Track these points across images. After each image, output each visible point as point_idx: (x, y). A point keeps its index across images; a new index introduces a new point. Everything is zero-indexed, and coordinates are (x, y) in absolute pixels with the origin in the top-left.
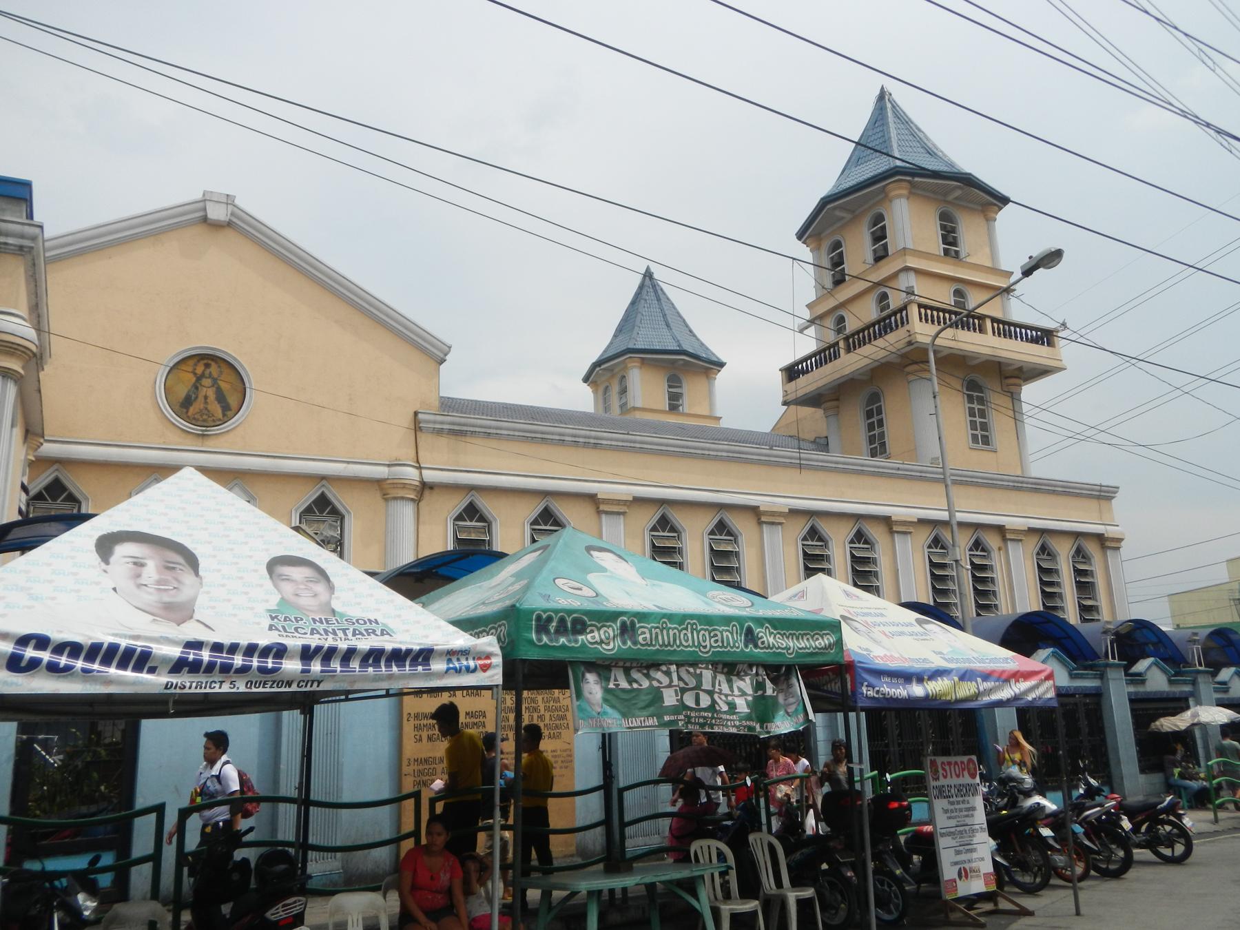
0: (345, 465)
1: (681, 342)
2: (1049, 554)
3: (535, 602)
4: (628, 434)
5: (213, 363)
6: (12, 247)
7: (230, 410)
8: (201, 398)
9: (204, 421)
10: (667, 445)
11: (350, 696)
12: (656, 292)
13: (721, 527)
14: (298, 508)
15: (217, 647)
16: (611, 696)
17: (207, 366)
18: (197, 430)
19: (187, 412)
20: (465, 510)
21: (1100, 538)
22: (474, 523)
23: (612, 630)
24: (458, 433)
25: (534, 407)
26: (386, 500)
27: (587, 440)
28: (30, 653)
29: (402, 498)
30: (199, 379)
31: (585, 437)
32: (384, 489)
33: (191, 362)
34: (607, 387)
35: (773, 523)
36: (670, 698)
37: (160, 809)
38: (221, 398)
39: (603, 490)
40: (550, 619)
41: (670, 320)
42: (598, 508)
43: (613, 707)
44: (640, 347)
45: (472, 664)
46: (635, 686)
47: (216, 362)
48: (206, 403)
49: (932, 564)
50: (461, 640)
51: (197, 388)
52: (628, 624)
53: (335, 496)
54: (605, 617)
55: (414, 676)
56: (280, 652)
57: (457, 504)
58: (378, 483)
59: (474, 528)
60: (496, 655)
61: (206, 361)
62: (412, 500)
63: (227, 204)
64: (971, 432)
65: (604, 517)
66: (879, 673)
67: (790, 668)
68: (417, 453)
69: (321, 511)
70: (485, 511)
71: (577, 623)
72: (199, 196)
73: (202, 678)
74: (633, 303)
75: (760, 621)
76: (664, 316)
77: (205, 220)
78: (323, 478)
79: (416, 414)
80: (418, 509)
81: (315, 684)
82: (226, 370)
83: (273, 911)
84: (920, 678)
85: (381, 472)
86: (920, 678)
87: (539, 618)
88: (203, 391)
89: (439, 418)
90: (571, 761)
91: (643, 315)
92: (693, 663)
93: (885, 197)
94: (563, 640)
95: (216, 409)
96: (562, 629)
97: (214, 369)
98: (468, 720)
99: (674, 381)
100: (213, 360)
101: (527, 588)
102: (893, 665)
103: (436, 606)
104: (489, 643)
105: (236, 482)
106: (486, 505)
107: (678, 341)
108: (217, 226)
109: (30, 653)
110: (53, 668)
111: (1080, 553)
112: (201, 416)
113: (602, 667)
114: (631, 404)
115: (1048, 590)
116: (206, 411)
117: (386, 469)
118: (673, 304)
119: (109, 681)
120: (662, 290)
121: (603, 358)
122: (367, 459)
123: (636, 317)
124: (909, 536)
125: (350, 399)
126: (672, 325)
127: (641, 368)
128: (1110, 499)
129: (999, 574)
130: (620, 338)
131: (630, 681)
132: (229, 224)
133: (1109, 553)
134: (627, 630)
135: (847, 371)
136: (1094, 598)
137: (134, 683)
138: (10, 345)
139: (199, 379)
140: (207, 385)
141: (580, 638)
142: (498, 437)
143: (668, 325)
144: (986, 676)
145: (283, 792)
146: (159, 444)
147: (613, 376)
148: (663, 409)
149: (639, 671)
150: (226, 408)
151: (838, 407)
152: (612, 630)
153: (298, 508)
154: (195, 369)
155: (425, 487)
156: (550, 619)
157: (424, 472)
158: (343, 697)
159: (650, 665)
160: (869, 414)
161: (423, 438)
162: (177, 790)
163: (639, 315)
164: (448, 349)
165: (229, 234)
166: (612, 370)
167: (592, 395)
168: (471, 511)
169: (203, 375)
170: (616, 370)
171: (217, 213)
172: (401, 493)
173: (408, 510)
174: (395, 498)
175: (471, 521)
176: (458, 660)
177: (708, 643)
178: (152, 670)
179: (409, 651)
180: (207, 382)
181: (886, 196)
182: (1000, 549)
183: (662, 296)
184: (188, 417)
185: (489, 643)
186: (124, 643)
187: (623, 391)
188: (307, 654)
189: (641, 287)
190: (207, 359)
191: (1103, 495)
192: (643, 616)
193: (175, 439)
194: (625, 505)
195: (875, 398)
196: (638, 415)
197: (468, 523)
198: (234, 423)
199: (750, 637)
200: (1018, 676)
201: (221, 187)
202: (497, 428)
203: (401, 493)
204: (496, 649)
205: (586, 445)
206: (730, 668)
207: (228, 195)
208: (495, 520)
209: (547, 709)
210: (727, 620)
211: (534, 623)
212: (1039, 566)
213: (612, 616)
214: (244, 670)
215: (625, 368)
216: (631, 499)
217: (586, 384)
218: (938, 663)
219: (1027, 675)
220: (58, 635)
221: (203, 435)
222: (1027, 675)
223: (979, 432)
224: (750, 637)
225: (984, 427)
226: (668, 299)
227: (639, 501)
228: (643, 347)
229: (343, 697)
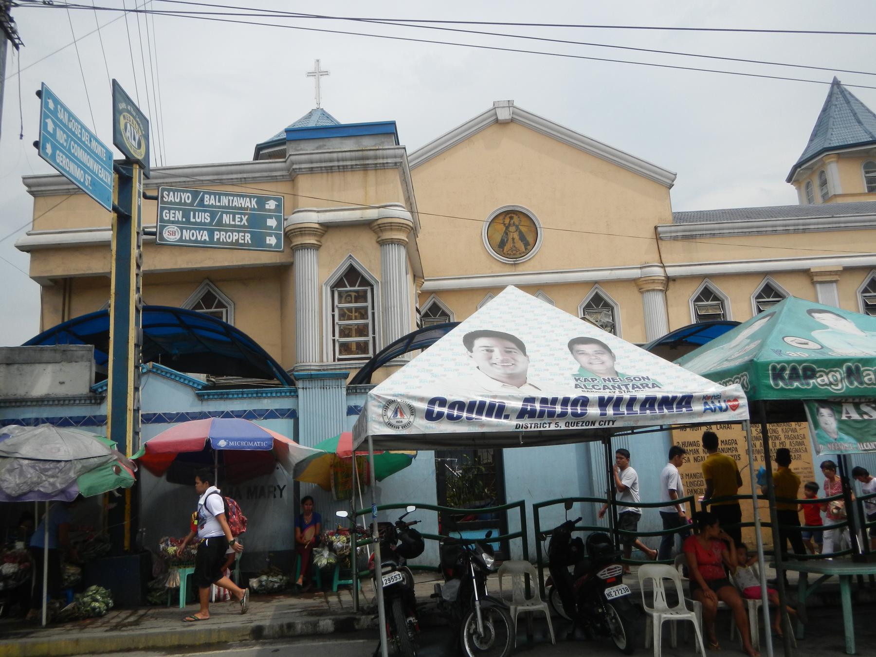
0: (609, 272)
1: (874, 133)
3: (769, 356)
4: (832, 217)
5: (514, 216)
6: (391, 165)
7: (529, 245)
8: (510, 240)
9: (514, 254)
10: (870, 221)
11: (635, 431)
12: (844, 96)
14: (582, 304)
15: (544, 401)
16: (845, 426)
17: (511, 218)
18: (511, 261)
19: (503, 251)
20: (702, 293)
22: (710, 303)
23: (839, 374)
24: (689, 237)
25: (748, 209)
26: (642, 293)
27: (796, 227)
28: (437, 409)
29: (654, 290)
30: (507, 228)
31: (794, 225)
32: (640, 285)
33: (501, 218)
34: (808, 183)
37: (522, 504)
38: (522, 238)
39: (814, 265)
40: (783, 369)
41: (861, 118)
42: (812, 279)
43: (847, 434)
44: (835, 145)
45: (723, 405)
46: (866, 417)
47: (517, 215)
48: (514, 242)
50: (713, 388)
51: (507, 234)
53: (607, 296)
55: (681, 415)
56: (584, 402)
57: (696, 289)
58: (635, 281)
59: (711, 306)
60: (742, 398)
61: (510, 215)
62: (661, 290)
63: (509, 107)
65: (818, 286)
68: (660, 256)
69: (597, 306)
70: (717, 292)
71: (808, 370)
72: (491, 106)
73: (537, 421)
74: (825, 110)
76: (855, 114)
77: (497, 121)
78: (596, 282)
79: (656, 228)
80: (666, 296)
81: (611, 423)
82: (524, 219)
83: (601, 572)
85: (636, 273)
87: (774, 368)
88: (510, 237)
89: (673, 228)
90: (812, 477)
91: (834, 118)
94: (796, 384)
95: (520, 245)
96: (794, 375)
97: (516, 220)
98: (723, 446)
100: (514, 214)
101: (761, 346)
103: (690, 364)
104: (735, 389)
105: (539, 292)
106: (717, 287)
107: (870, 133)
109: (437, 409)
110: (450, 417)
112: (512, 252)
113: (835, 403)
114: (832, 193)
116: (517, 250)
117: (639, 271)
118: (862, 103)
119: (483, 425)
120: (850, 93)
121: (802, 160)
122: (624, 265)
123: (828, 121)
125: (608, 225)
126: (862, 120)
127: (837, 162)
130: (815, 141)
131: (861, 413)
132: (512, 121)
137: (497, 425)
138: (398, 225)
139: (507, 228)
140: (513, 231)
141: (811, 381)
142: (722, 235)
143: (859, 122)
145: (597, 495)
146: (489, 273)
147: (813, 173)
148: (862, 191)
149: (868, 405)
150: (526, 244)
152: (839, 374)
153: (582, 304)
154: (504, 222)
155: (669, 280)
156: (783, 369)
157: (667, 269)
158: (630, 432)
162: (530, 492)
163: (832, 119)
164: (674, 176)
165: (512, 126)
166: (812, 168)
167: (796, 191)
168: (707, 294)
169: (509, 224)
170: (816, 167)
171: (503, 115)
172: (652, 287)
174: (648, 291)
175: (707, 301)
176: (713, 402)
178: (507, 417)
179: (674, 398)
180: (512, 229)
183: (850, 99)
184: (504, 253)
185: (735, 389)
186: (488, 401)
187: (824, 183)
188: (603, 403)
189: (831, 95)
193: (497, 269)
194: (836, 275)
196: (840, 201)
197: (705, 303)
198: (532, 254)
201: (504, 97)
202: (720, 229)
203: (652, 287)
204: (742, 393)
205: (796, 231)
207: (509, 101)
208: (727, 298)
209: (787, 437)
211: (770, 372)
213: (837, 363)
214: (563, 415)
215: (824, 164)
216: (841, 269)
217: (790, 184)
220: (451, 398)
221: (515, 264)
226: (857, 100)
227: (849, 270)
228: (838, 145)
229: (630, 432)
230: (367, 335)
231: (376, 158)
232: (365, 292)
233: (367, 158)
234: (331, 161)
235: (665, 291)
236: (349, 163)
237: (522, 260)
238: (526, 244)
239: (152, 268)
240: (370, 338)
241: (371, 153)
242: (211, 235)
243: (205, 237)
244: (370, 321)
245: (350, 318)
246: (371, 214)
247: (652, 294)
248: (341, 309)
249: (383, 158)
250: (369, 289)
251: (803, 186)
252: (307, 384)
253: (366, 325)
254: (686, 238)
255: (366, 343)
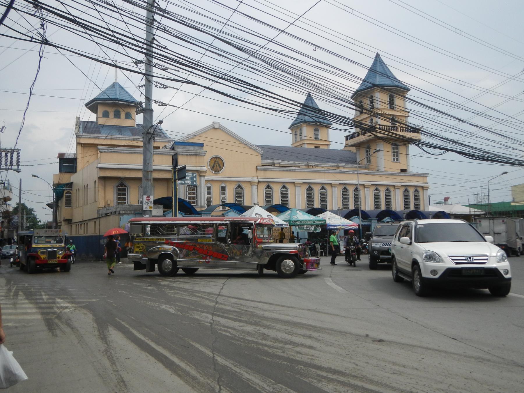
2: (407, 191)
3: (292, 219)
8: (216, 166)
12: (311, 101)
13: (323, 188)
17: (216, 159)
21: (422, 187)
30: (215, 162)
32: (251, 183)
33: (213, 159)
35: (335, 187)
36: (305, 228)
38: (219, 166)
49: (375, 195)
50: (284, 223)
52: (301, 221)
54: (299, 220)
57: (265, 186)
58: (250, 182)
64: (393, 157)
66: (330, 226)
67: (319, 225)
72: (212, 123)
75: (315, 220)
77: (214, 128)
78: (239, 181)
79: (257, 167)
84: (336, 226)
85: (250, 180)
86: (336, 226)
88: (216, 165)
92: (308, 225)
93: (373, 91)
96: (294, 222)
97: (218, 160)
99: (317, 130)
101: (290, 217)
102: (332, 224)
103: (279, 217)
104: (287, 223)
106: (272, 185)
108: (216, 129)
111: (416, 191)
113: (298, 225)
115: (406, 200)
116: (217, 169)
117: (251, 179)
121: (295, 123)
124: (369, 189)
127: (306, 127)
128: (426, 176)
129: (393, 197)
132: (219, 128)
133: (425, 191)
134: (301, 222)
135: (361, 140)
136: (419, 202)
142: (274, 170)
144: (346, 226)
150: (220, 168)
151: (359, 148)
155: (259, 182)
159: (303, 225)
160: (367, 151)
161: (259, 172)
165: (218, 130)
170: (299, 127)
171: (216, 126)
173: (256, 187)
177: (309, 223)
180: (216, 163)
181: (374, 91)
182: (393, 191)
185: (287, 223)
189: (307, 99)
190: (216, 158)
191: (425, 176)
192: (302, 220)
195: (368, 147)
199: (314, 222)
200: (352, 225)
205: (292, 171)
206: (312, 225)
210: (311, 220)
212: (404, 195)
213: (299, 220)
218: (340, 224)
219: (353, 225)
222: (353, 225)
223: (395, 158)
224: (314, 222)
225: (397, 156)
226: (315, 103)
227: (304, 183)
230: (195, 199)
231: (200, 153)
232: (195, 188)
233: (197, 153)
234: (188, 153)
235: (257, 185)
236: (192, 154)
237: (219, 173)
238: (220, 168)
239: (136, 177)
240: (196, 200)
241: (199, 152)
242: (184, 182)
243: (183, 182)
244: (196, 196)
245: (191, 195)
246: (198, 168)
247: (254, 186)
248: (188, 192)
249: (201, 153)
250: (196, 187)
251: (294, 132)
252: (204, 215)
253: (195, 197)
254: (264, 170)
255: (195, 201)
